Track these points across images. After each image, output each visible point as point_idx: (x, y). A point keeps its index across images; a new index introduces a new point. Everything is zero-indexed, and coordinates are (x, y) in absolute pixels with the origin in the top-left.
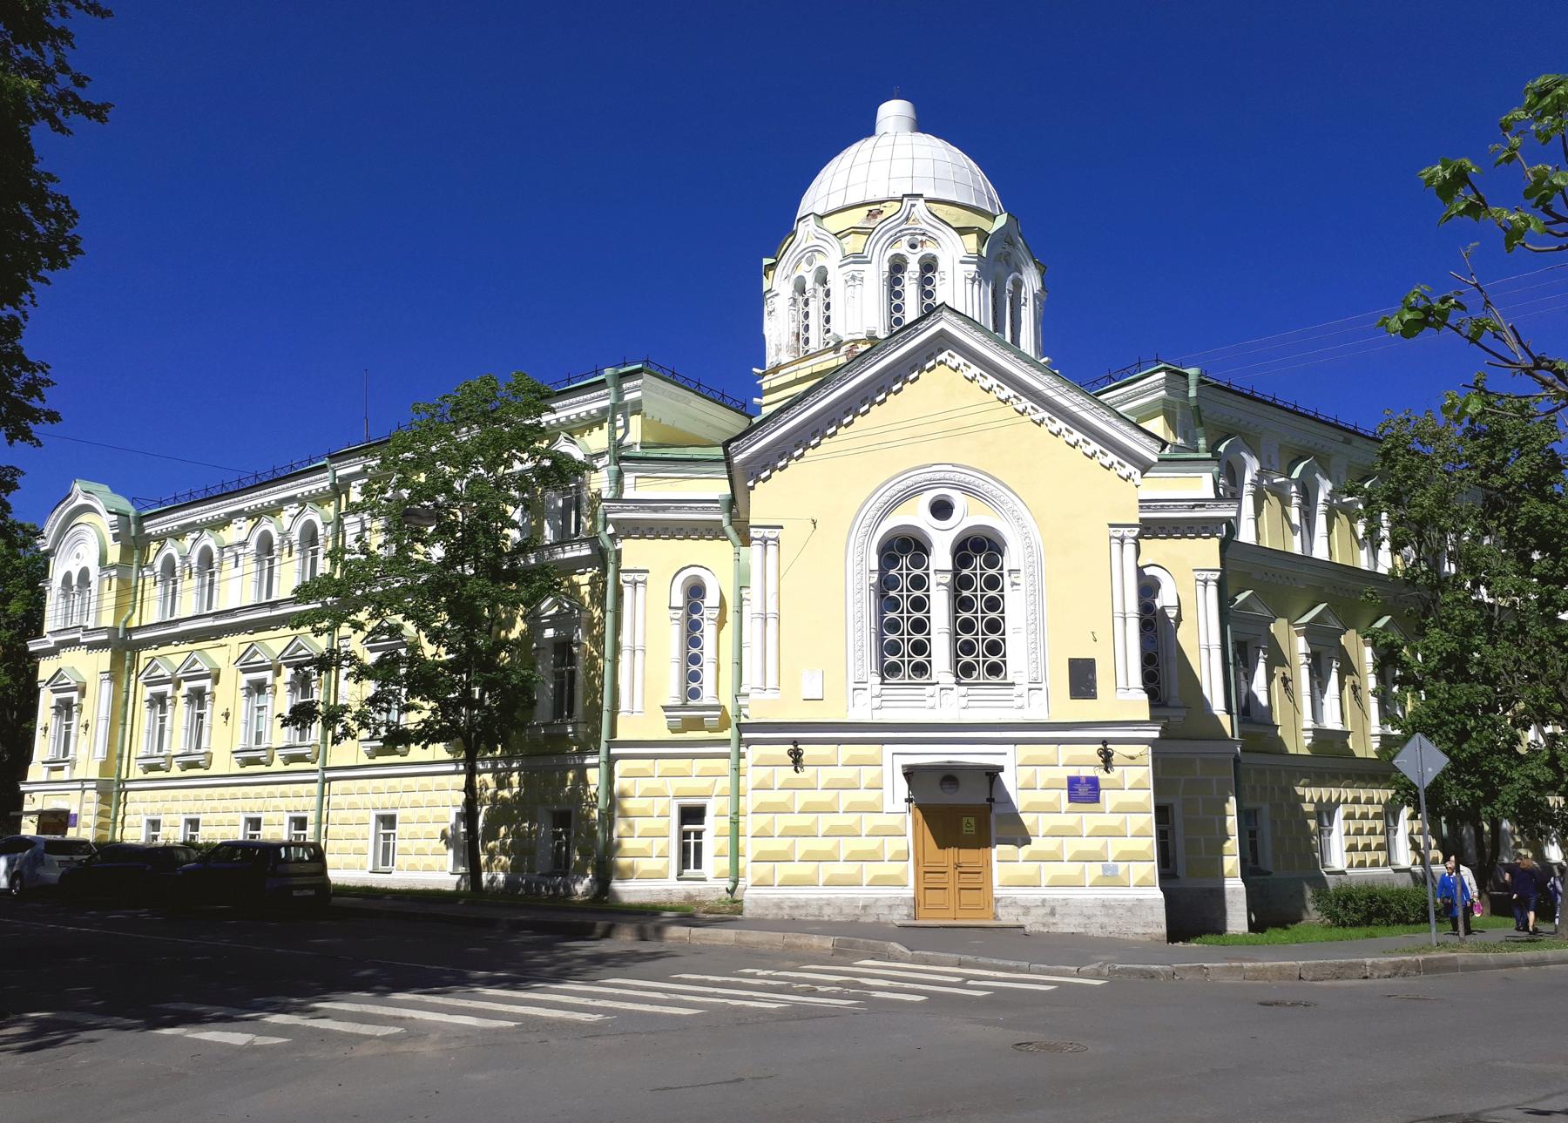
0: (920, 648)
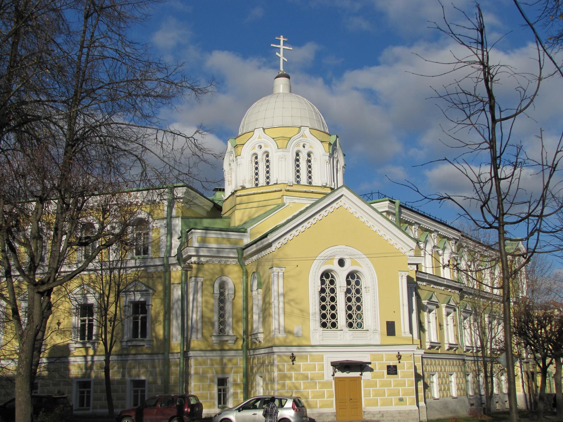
0: (333, 316)
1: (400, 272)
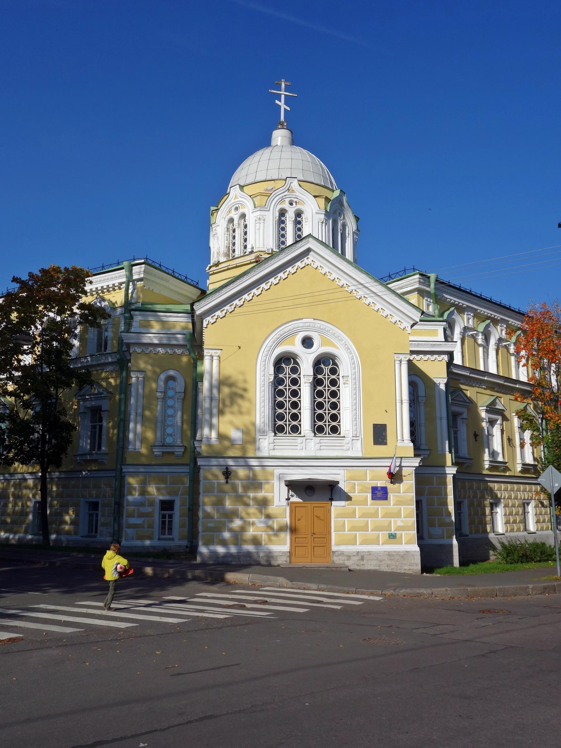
0: (295, 417)
1: (396, 356)
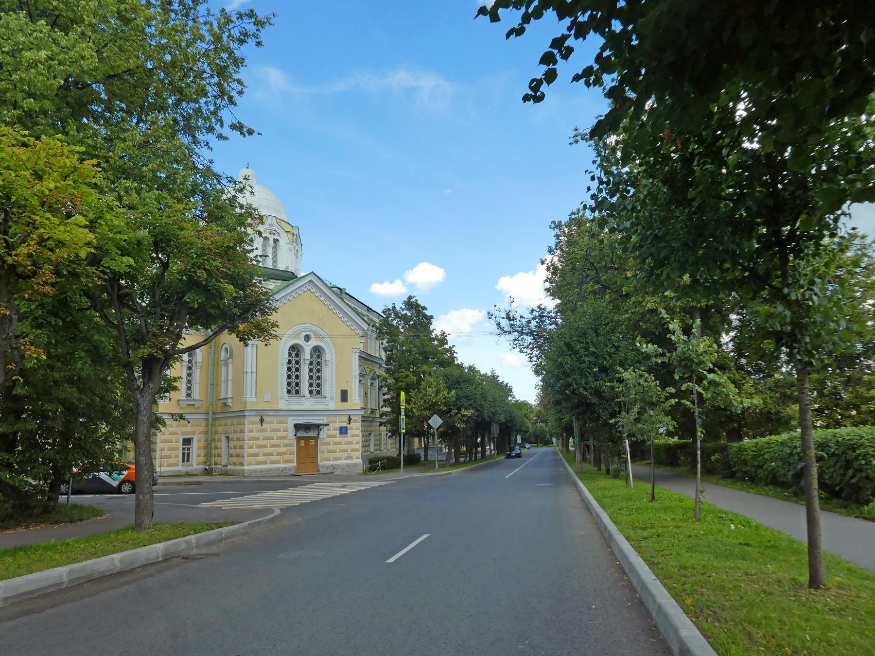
0: (297, 384)
